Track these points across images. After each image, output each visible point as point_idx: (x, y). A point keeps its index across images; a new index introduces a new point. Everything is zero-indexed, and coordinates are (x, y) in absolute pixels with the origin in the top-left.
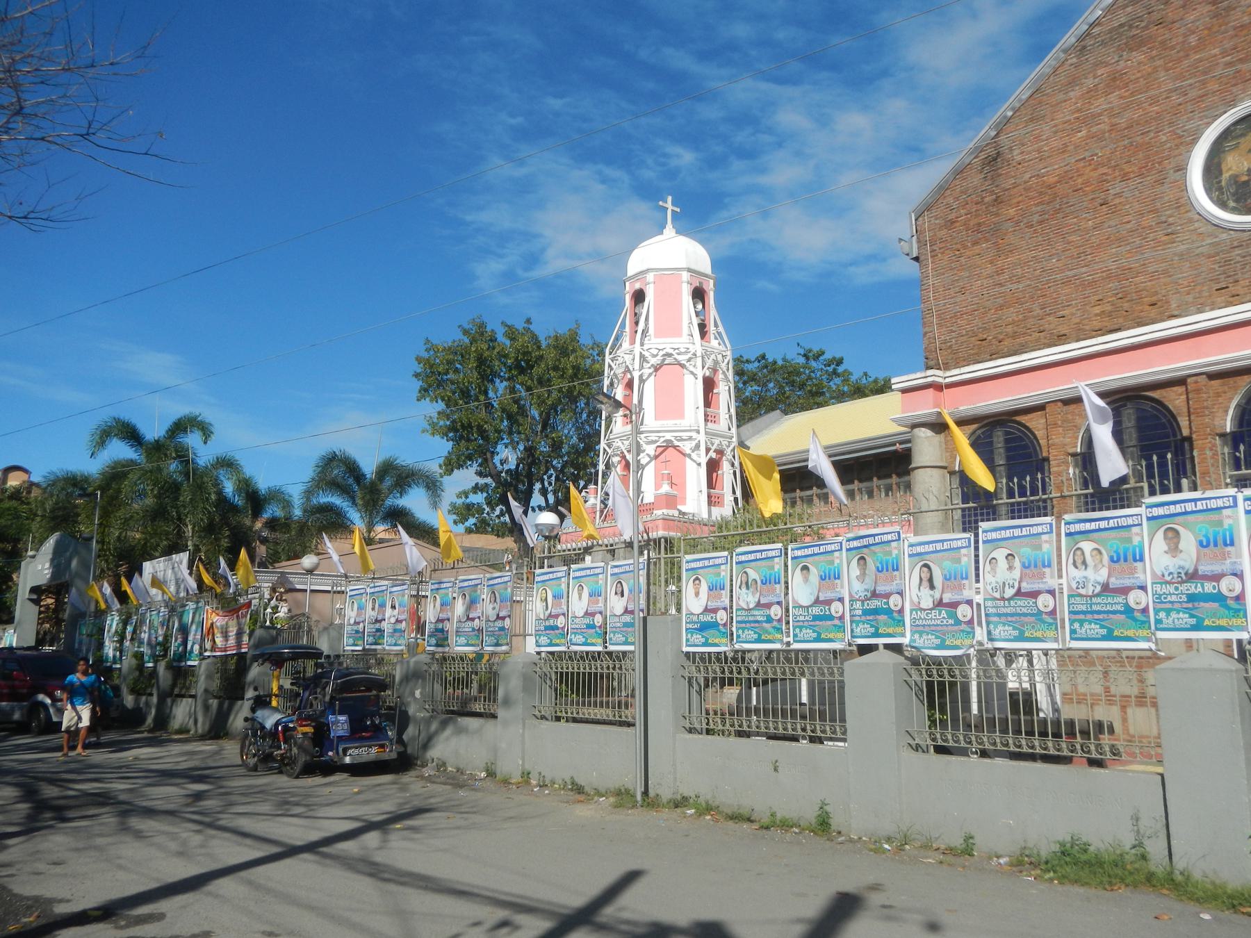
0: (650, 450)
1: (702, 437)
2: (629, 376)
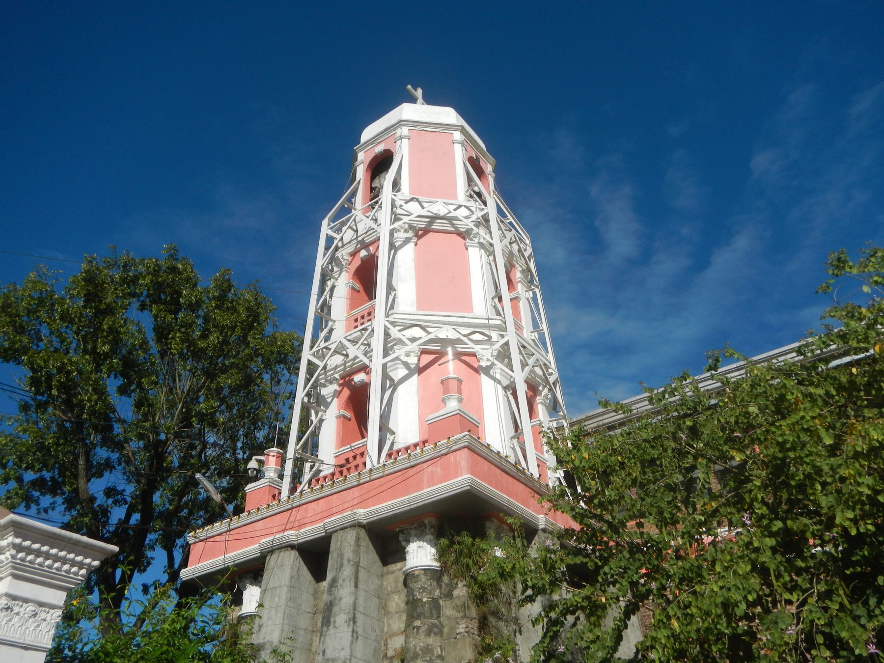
0: (409, 354)
1: (511, 337)
2: (363, 253)
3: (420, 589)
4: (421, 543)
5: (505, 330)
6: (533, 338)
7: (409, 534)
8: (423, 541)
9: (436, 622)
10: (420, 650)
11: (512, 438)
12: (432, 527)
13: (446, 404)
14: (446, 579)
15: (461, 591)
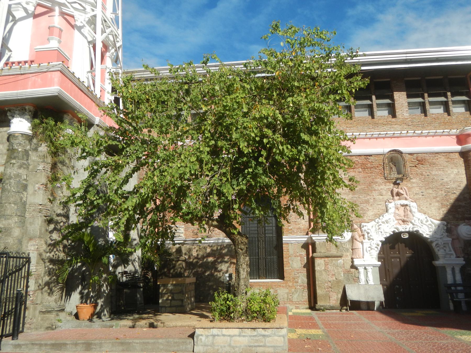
3: (18, 144)
4: (22, 119)
5: (96, 7)
6: (112, 17)
7: (15, 113)
8: (23, 118)
9: (25, 162)
10: (13, 175)
11: (88, 72)
12: (30, 111)
13: (49, 42)
14: (35, 141)
15: (44, 148)
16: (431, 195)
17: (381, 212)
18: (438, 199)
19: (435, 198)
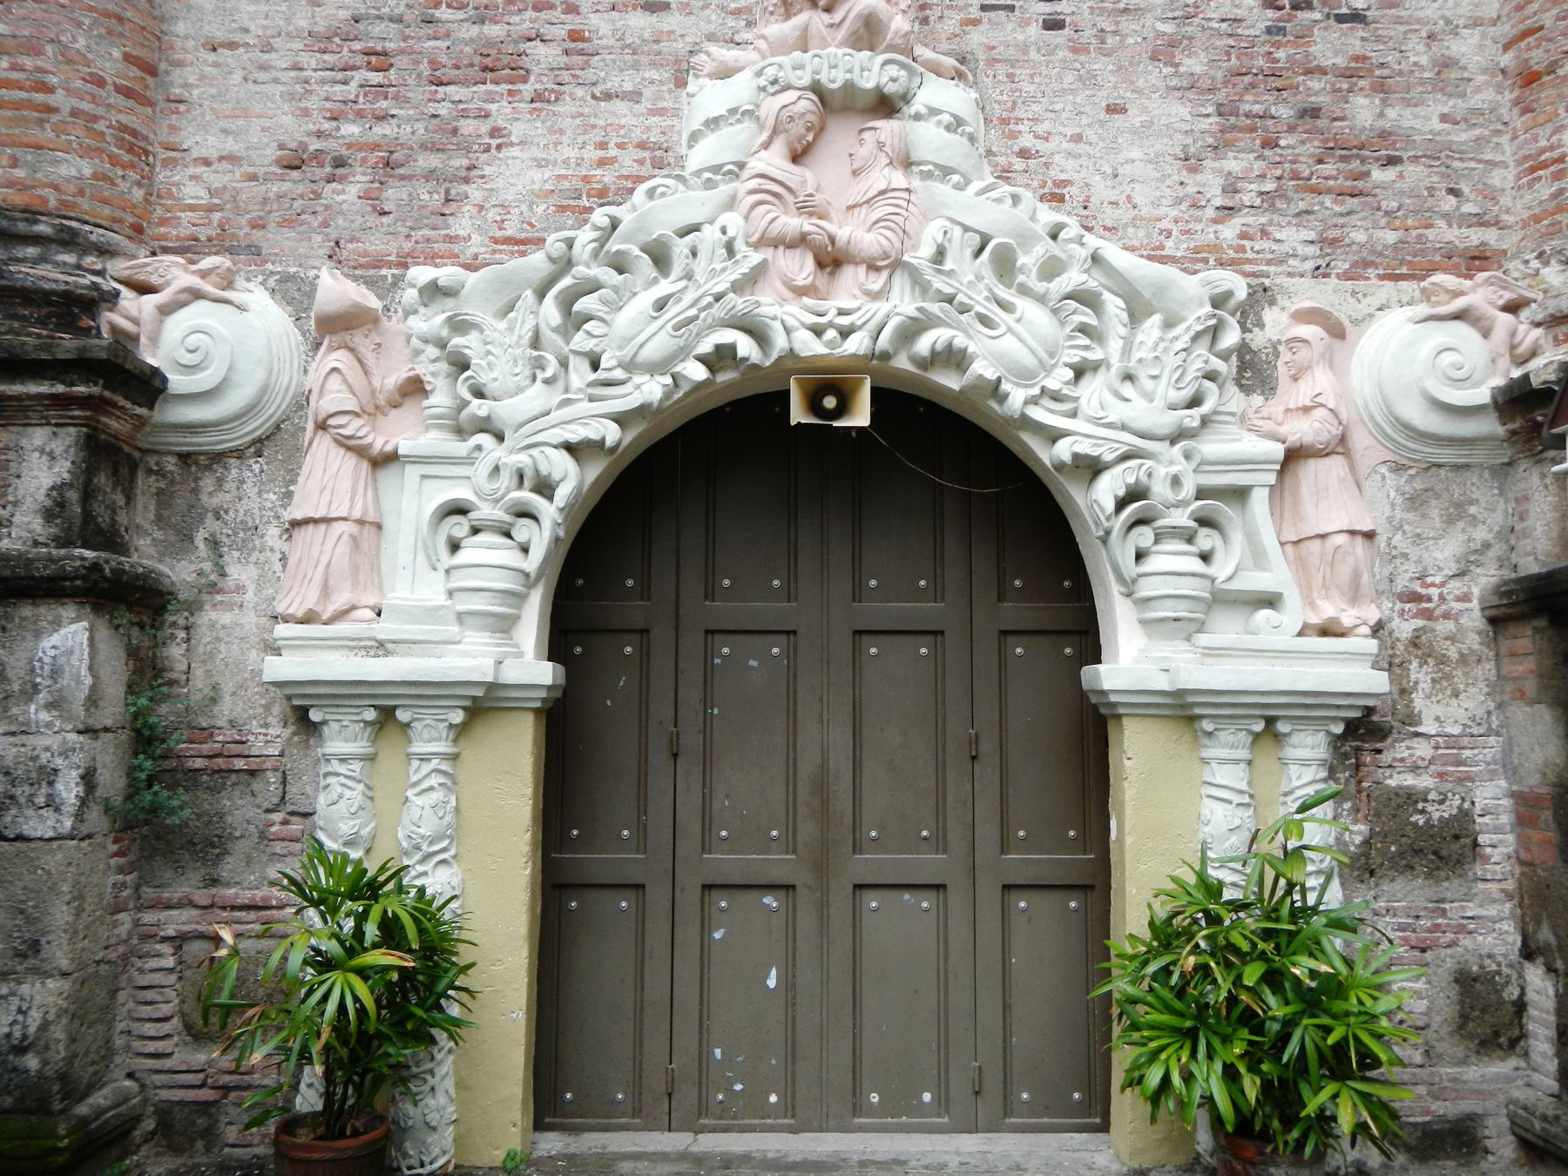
16: (1127, 25)
17: (628, 162)
18: (1194, 64)
19: (1165, 51)
